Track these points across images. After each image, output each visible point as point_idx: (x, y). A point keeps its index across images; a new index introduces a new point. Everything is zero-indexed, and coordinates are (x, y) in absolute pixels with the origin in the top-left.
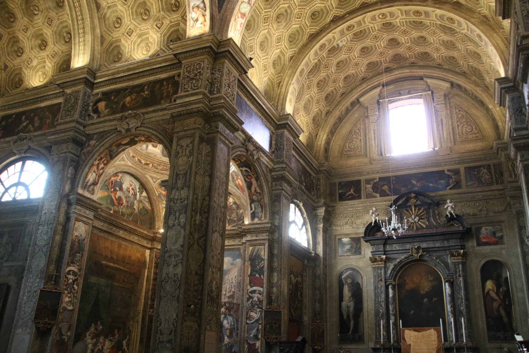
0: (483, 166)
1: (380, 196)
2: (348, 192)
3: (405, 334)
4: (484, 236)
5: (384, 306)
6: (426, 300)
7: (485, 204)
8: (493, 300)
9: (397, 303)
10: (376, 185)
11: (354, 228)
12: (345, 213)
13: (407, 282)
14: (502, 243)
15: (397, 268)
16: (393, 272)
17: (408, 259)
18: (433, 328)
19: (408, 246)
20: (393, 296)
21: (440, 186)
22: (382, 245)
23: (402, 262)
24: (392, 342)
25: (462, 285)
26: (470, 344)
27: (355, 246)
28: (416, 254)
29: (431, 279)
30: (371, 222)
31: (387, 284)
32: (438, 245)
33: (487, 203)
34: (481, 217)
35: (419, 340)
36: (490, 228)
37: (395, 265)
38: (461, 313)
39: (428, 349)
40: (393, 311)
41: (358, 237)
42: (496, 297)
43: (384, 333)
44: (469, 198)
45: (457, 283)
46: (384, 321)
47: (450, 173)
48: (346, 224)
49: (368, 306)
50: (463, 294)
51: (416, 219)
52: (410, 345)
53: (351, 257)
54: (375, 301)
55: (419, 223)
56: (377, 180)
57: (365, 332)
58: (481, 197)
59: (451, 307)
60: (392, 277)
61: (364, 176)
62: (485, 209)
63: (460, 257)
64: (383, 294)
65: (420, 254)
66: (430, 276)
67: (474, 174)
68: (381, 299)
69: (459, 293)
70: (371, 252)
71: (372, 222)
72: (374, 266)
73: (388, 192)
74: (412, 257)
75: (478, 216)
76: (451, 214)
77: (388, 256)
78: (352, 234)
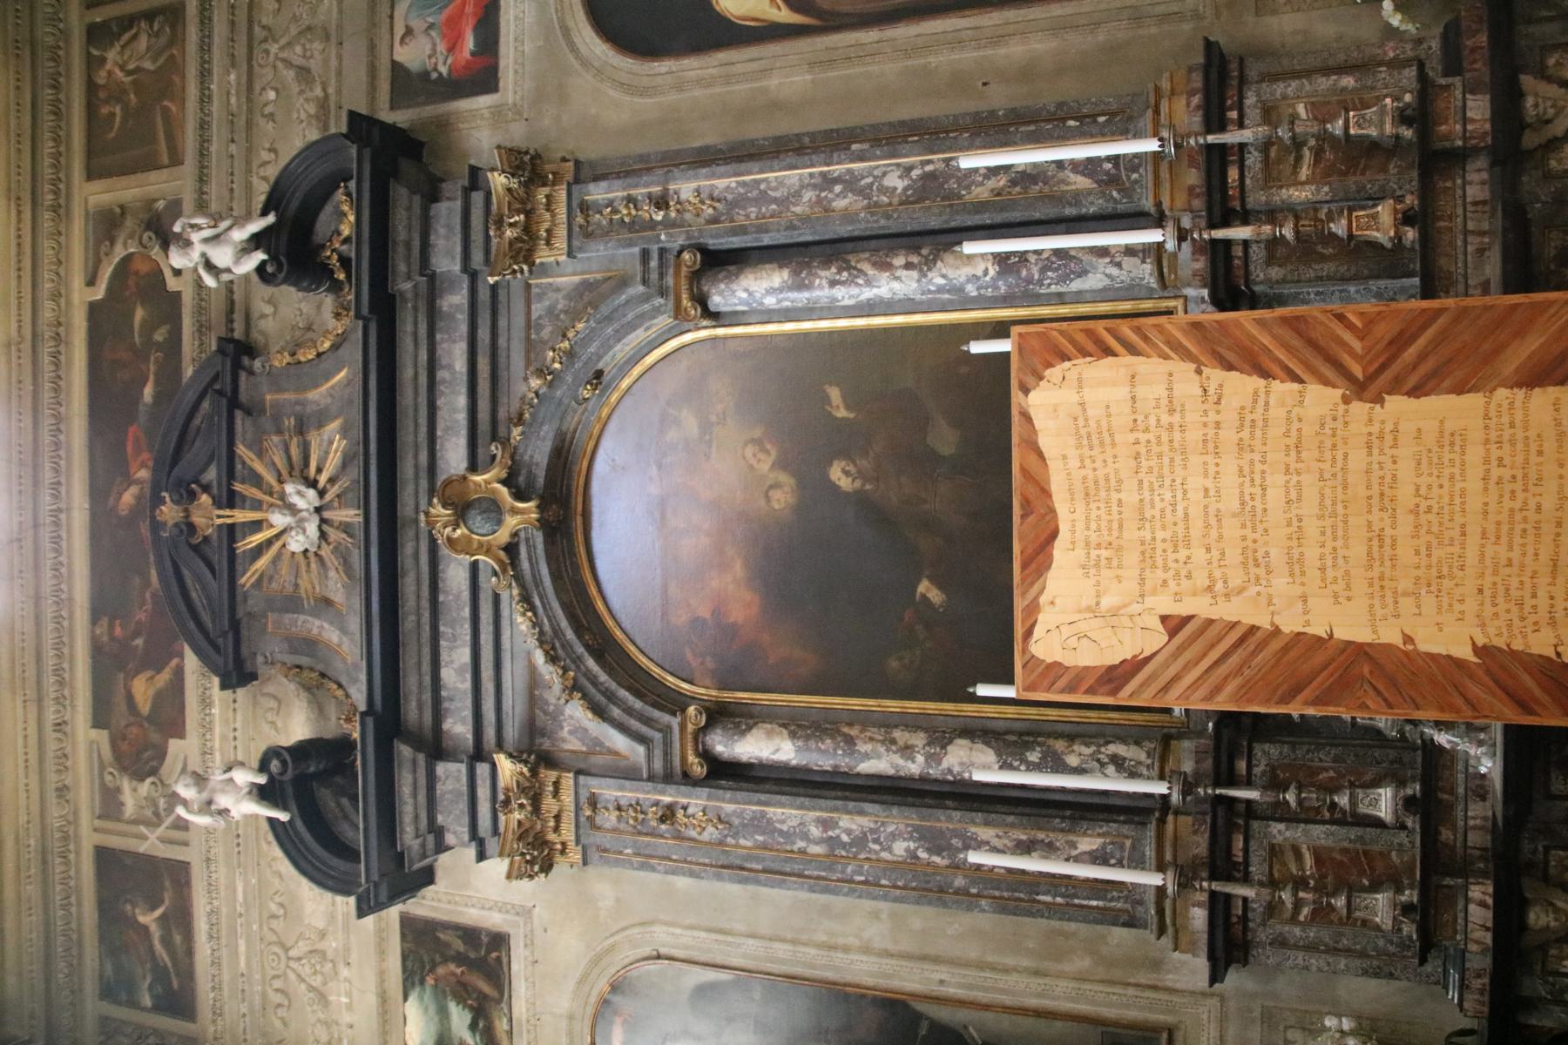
0: (93, 64)
1: (181, 735)
2: (151, 946)
3: (1069, 660)
4: (441, 47)
6: (840, 476)
7: (274, 48)
9: (855, 703)
10: (124, 746)
11: (347, 950)
12: (264, 995)
13: (704, 612)
15: (594, 682)
16: (616, 712)
17: (538, 582)
18: (1016, 396)
19: (456, 575)
20: (793, 736)
21: (159, 336)
22: (441, 768)
23: (557, 632)
24: (1160, 788)
25: (724, 183)
26: (1185, 112)
27: (452, 967)
28: (499, 522)
30: (265, 826)
31: (699, 770)
32: (455, 356)
33: (271, 34)
34: (339, 73)
35: (1131, 534)
37: (574, 688)
38: (929, 187)
39: (1211, 446)
40: (907, 751)
41: (403, 936)
43: (1087, 844)
44: (233, 148)
45: (714, 220)
46: (986, 833)
47: (107, 272)
48: (322, 998)
49: (866, 950)
50: (793, 176)
51: (301, 503)
52: (1174, 625)
53: (520, 1007)
54: (821, 884)
55: (323, 479)
56: (102, 736)
57: (1083, 1008)
58: (233, 77)
59: (885, 266)
60: (648, 721)
61: (75, 822)
62: (298, 49)
63: (541, 195)
64: (775, 812)
65: (504, 490)
67: (125, 119)
68: (805, 836)
69: (783, 202)
70: (481, 856)
71: (271, 820)
72: (575, 855)
73: (165, 676)
74: (523, 550)
75: (331, 90)
76: (257, 241)
77: (511, 732)
78: (382, 976)
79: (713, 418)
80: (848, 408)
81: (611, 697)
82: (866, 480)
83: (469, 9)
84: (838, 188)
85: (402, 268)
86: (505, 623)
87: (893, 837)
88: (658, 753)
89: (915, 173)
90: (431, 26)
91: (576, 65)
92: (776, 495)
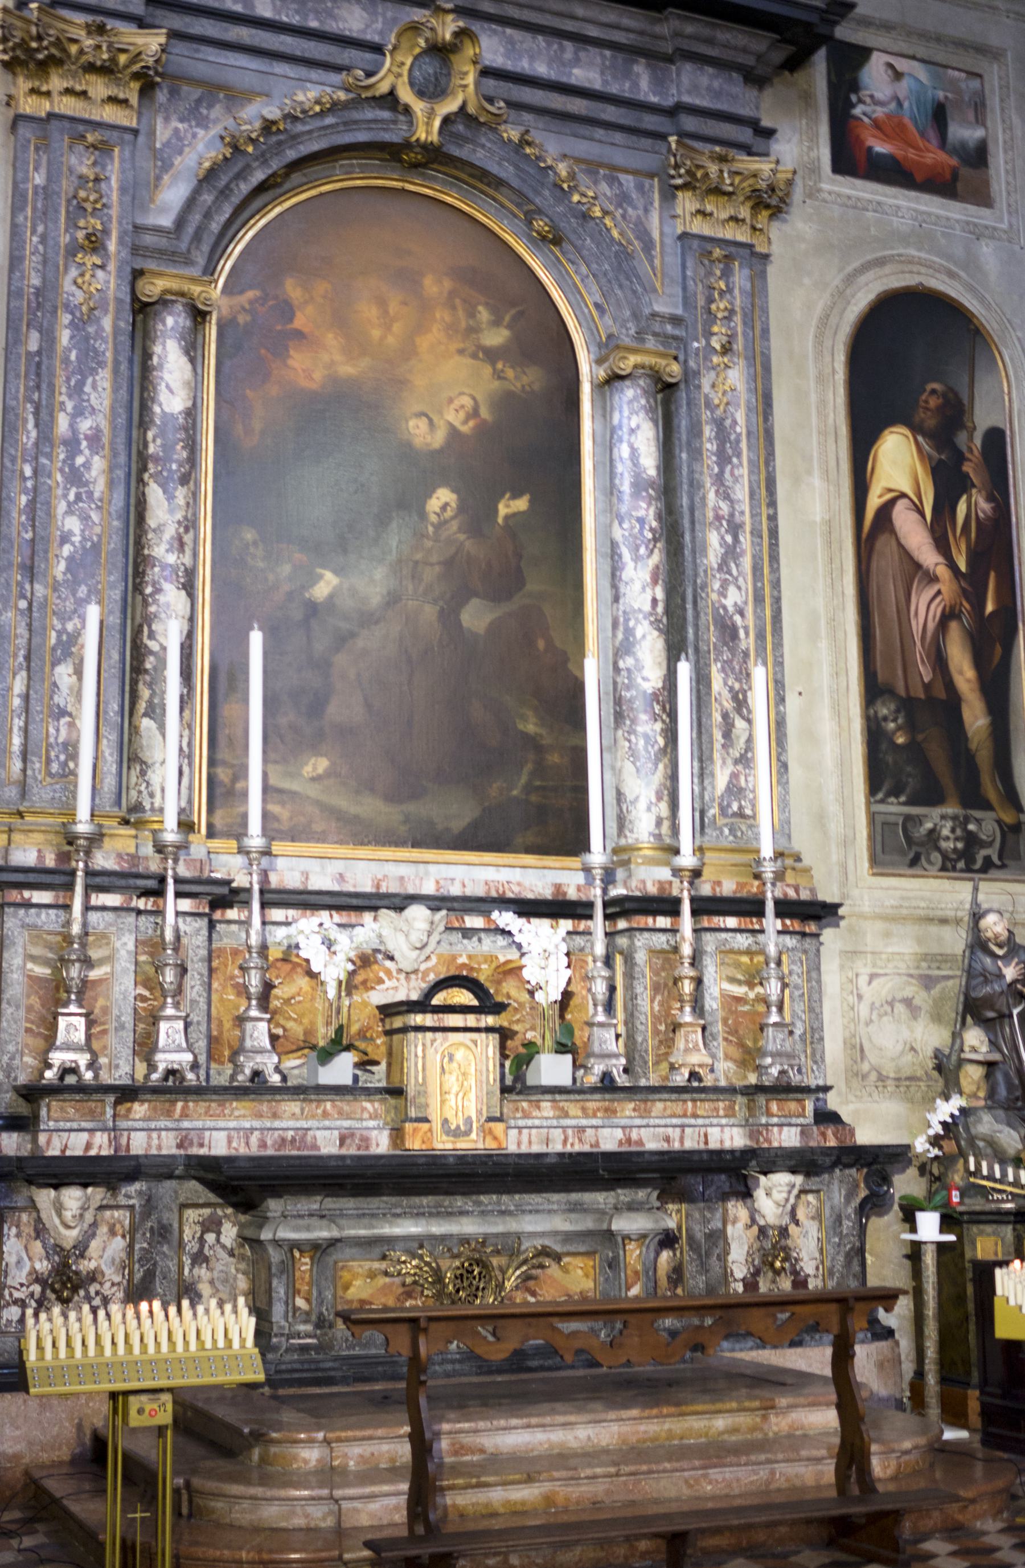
4: (879, 112)
5: (99, 488)
8: (913, 569)
13: (300, 322)
14: (982, 197)
15: (241, 176)
17: (349, 125)
23: (295, 139)
29: (496, 337)
36: (921, 72)
42: (929, 557)
60: (197, 237)
64: (104, 378)
65: (451, 106)
66: (484, 314)
68: (79, 412)
74: (386, 114)
79: (500, 366)
80: (507, 517)
81: (224, 193)
82: (439, 526)
83: (912, 154)
84: (729, 539)
85: (689, 29)
86: (302, 71)
87: (85, 518)
88: (163, 242)
89: (737, 618)
90: (900, 104)
91: (849, 269)
92: (423, 424)
